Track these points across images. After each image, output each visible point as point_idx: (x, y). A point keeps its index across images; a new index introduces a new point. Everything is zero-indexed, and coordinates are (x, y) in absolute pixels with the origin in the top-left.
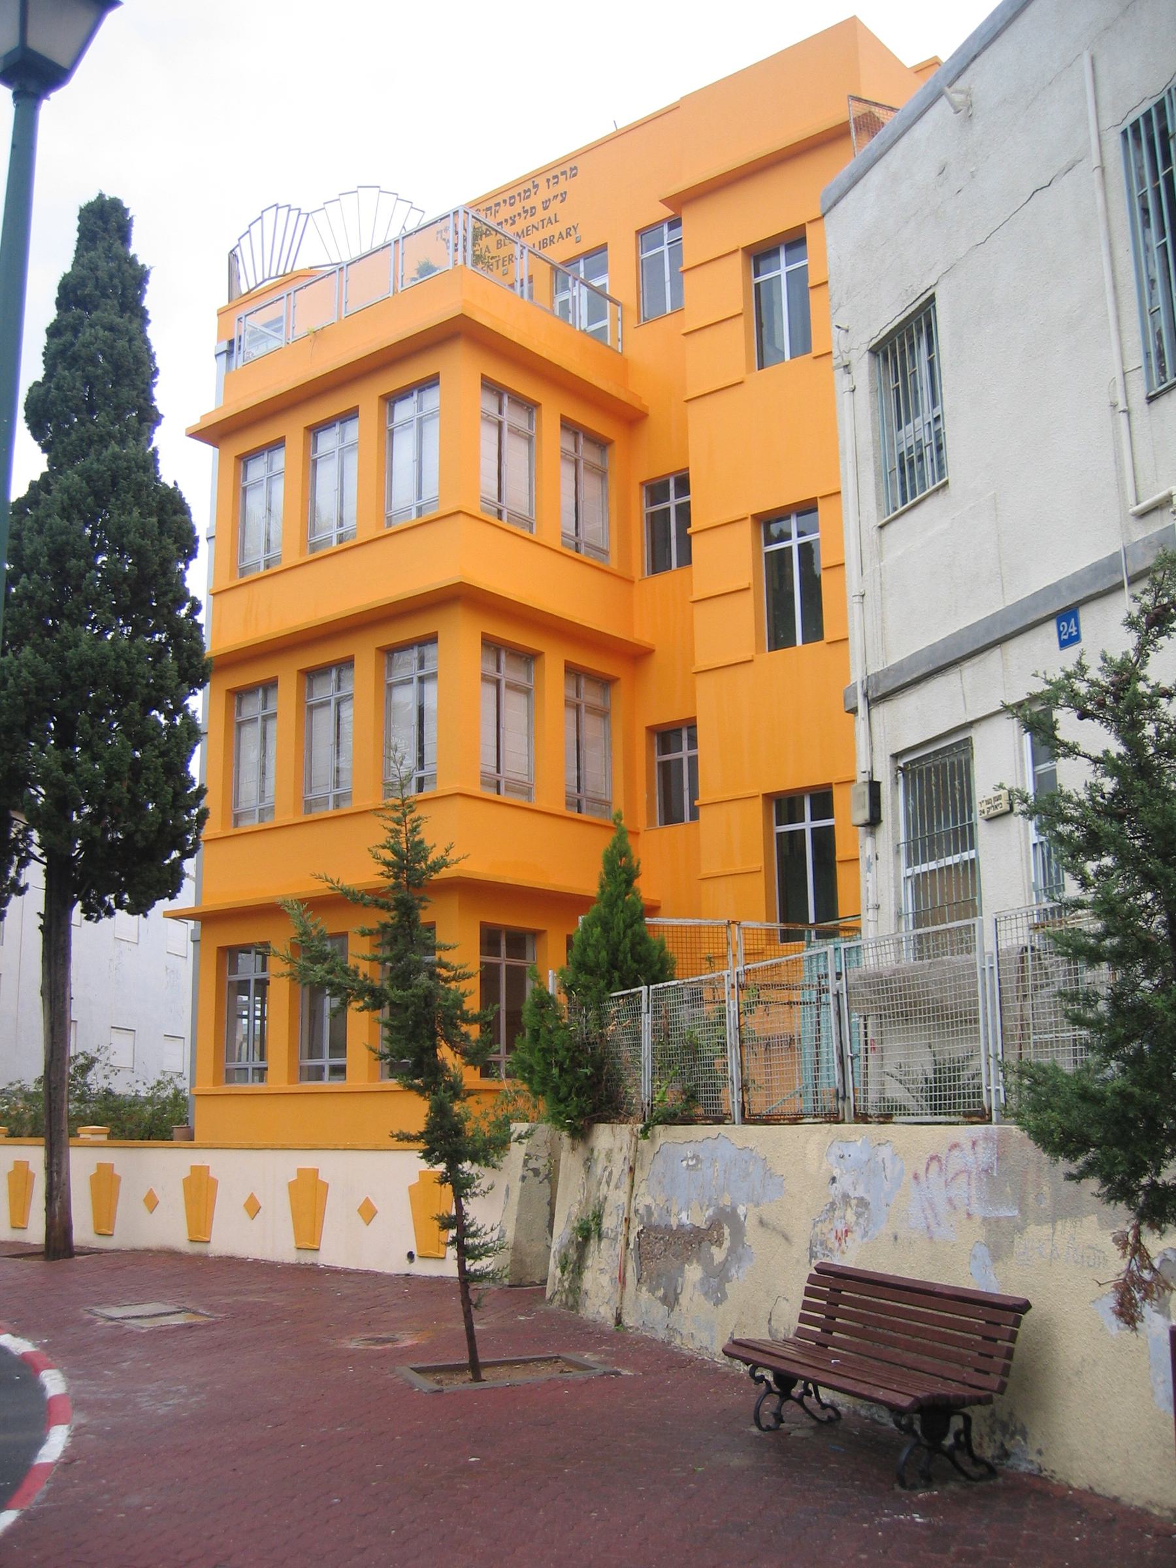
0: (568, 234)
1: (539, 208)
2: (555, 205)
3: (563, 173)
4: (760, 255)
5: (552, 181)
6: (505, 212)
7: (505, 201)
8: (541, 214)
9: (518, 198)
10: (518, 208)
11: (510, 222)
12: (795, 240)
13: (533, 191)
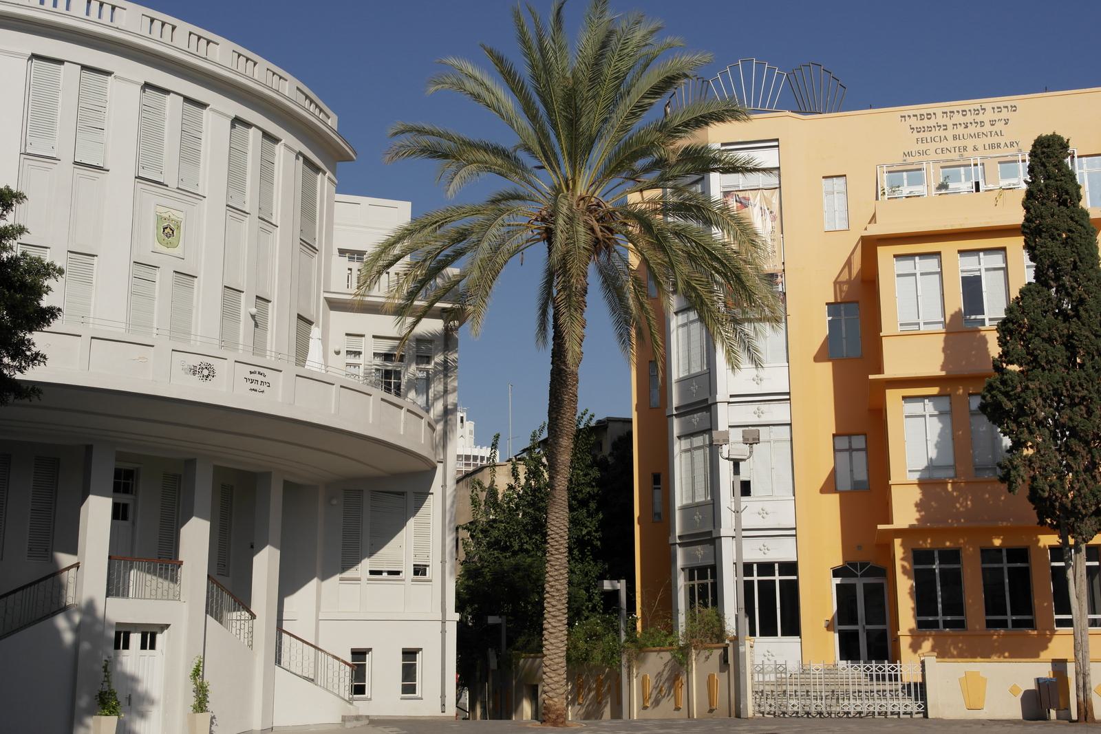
0: (1012, 145)
1: (987, 124)
2: (999, 126)
3: (1007, 107)
5: (996, 110)
7: (958, 112)
8: (987, 128)
9: (969, 113)
11: (963, 126)
13: (981, 112)
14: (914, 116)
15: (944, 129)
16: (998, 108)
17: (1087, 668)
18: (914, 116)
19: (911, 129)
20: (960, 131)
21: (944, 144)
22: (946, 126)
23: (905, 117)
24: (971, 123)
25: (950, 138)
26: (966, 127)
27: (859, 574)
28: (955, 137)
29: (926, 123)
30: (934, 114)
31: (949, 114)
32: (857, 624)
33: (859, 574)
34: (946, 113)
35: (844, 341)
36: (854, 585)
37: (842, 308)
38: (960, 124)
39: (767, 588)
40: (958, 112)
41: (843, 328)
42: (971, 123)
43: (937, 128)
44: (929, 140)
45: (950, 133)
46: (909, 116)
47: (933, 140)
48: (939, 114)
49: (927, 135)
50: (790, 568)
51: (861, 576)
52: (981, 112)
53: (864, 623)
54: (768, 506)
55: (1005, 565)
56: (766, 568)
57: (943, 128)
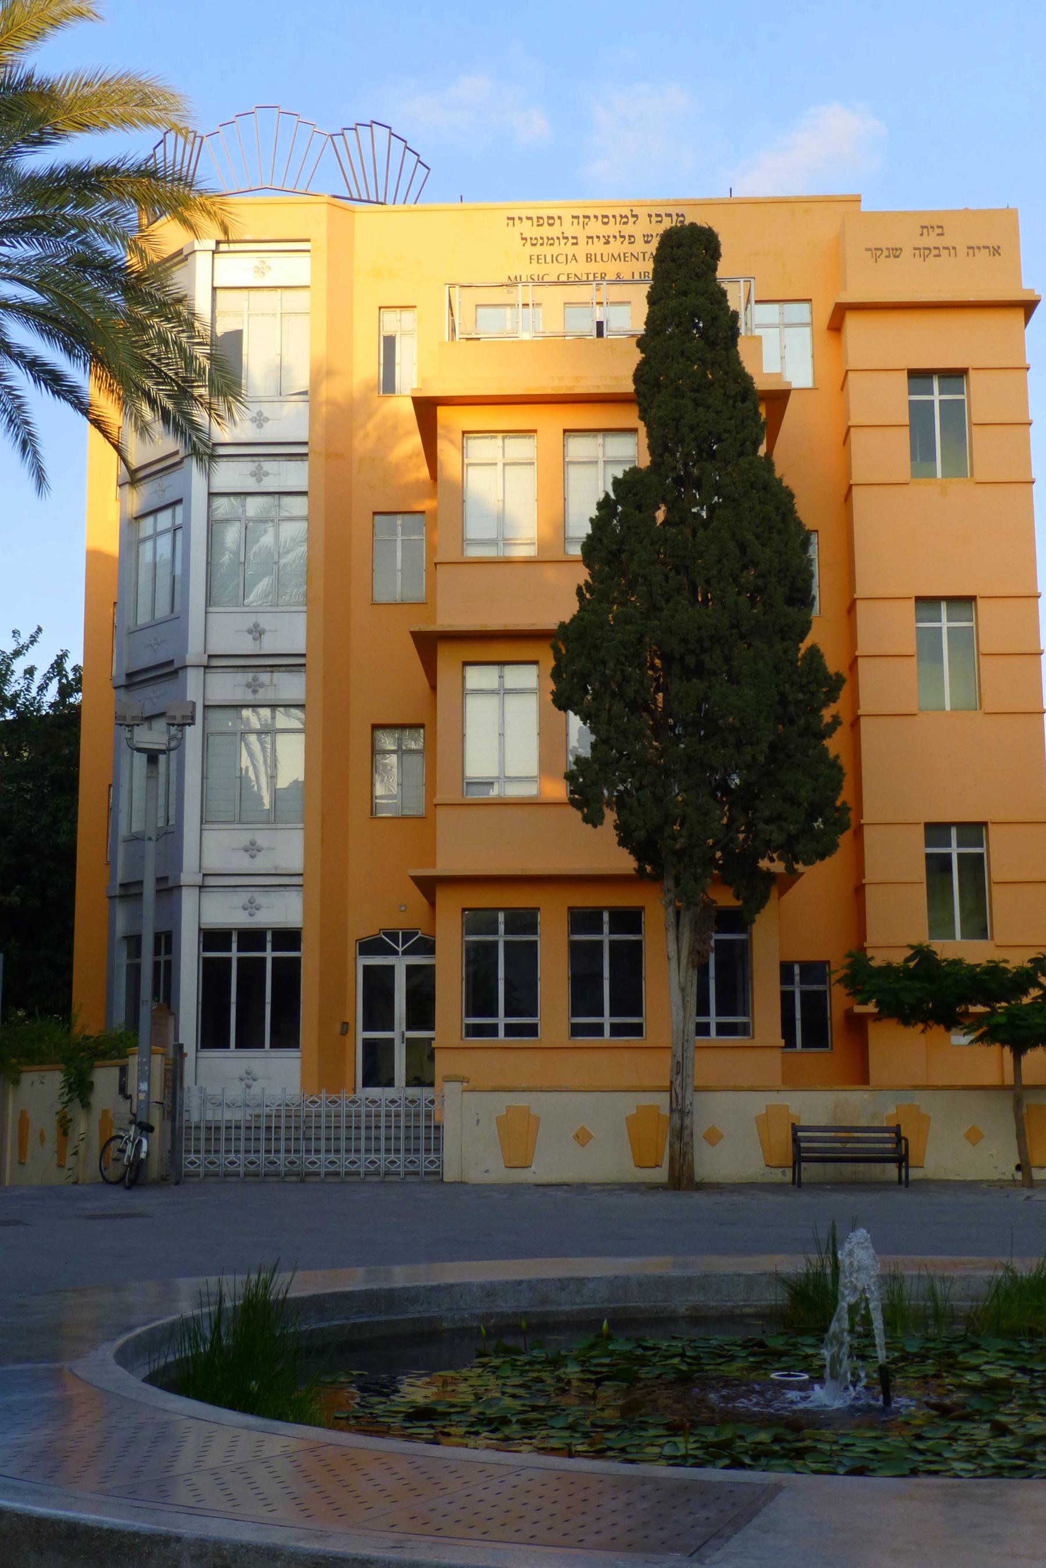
1: (639, 240)
4: (919, 376)
5: (654, 219)
6: (595, 228)
7: (596, 217)
9: (612, 220)
10: (612, 229)
11: (603, 240)
12: (955, 376)
14: (528, 218)
15: (573, 244)
16: (657, 215)
17: (688, 1102)
18: (528, 218)
19: (523, 239)
20: (598, 247)
21: (573, 268)
22: (575, 238)
23: (513, 219)
24: (615, 237)
25: (582, 258)
26: (607, 242)
27: (400, 949)
28: (589, 258)
29: (546, 231)
30: (560, 218)
31: (581, 219)
32: (392, 1030)
33: (400, 949)
34: (577, 217)
35: (399, 574)
36: (391, 968)
37: (399, 522)
38: (598, 237)
39: (251, 970)
40: (596, 217)
41: (399, 553)
42: (615, 237)
43: (563, 241)
44: (549, 259)
45: (581, 251)
46: (520, 219)
47: (555, 259)
48: (567, 219)
49: (547, 250)
50: (288, 938)
51: (404, 953)
52: (632, 220)
53: (404, 1029)
54: (262, 838)
55: (606, 937)
56: (252, 938)
57: (571, 241)
